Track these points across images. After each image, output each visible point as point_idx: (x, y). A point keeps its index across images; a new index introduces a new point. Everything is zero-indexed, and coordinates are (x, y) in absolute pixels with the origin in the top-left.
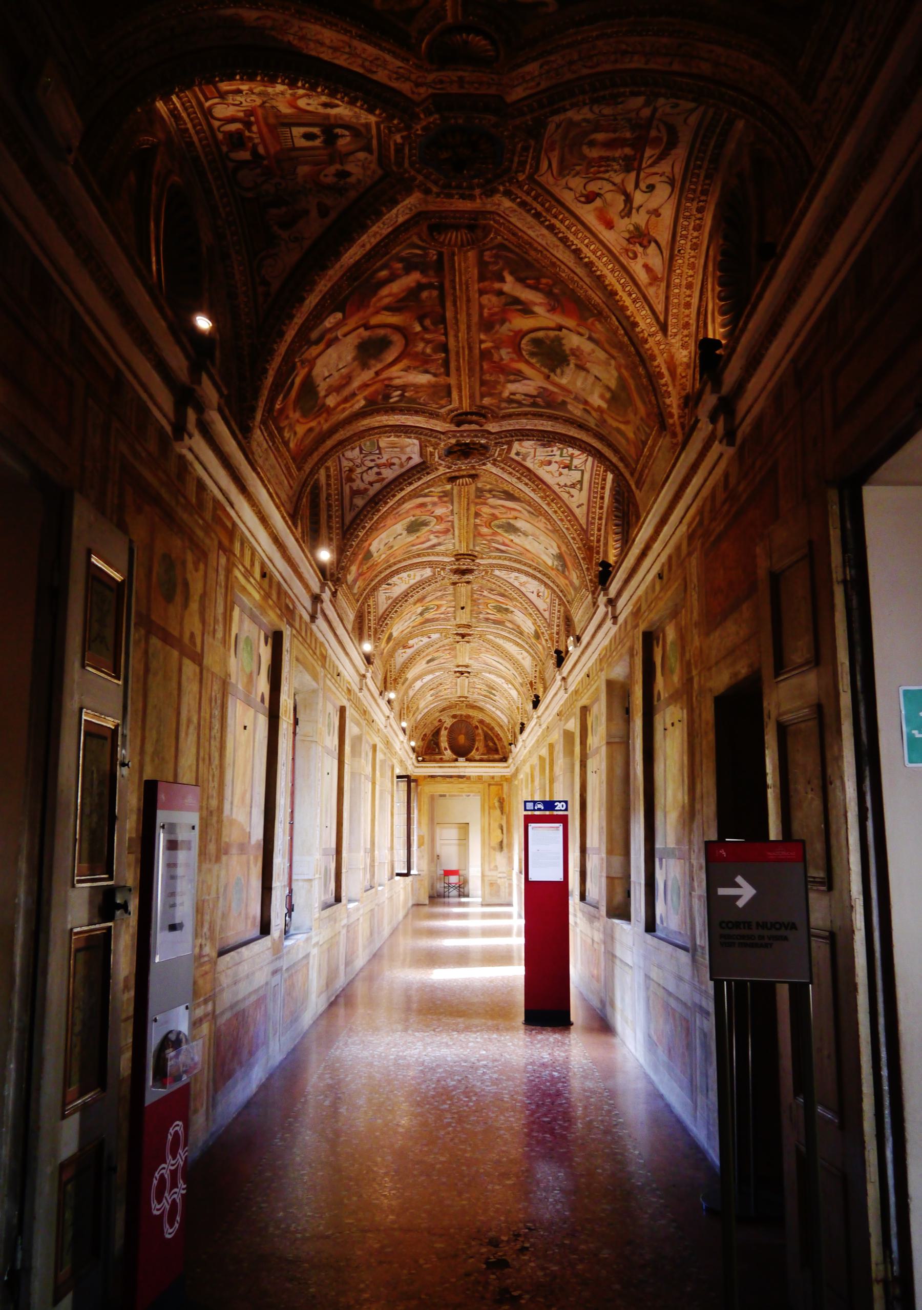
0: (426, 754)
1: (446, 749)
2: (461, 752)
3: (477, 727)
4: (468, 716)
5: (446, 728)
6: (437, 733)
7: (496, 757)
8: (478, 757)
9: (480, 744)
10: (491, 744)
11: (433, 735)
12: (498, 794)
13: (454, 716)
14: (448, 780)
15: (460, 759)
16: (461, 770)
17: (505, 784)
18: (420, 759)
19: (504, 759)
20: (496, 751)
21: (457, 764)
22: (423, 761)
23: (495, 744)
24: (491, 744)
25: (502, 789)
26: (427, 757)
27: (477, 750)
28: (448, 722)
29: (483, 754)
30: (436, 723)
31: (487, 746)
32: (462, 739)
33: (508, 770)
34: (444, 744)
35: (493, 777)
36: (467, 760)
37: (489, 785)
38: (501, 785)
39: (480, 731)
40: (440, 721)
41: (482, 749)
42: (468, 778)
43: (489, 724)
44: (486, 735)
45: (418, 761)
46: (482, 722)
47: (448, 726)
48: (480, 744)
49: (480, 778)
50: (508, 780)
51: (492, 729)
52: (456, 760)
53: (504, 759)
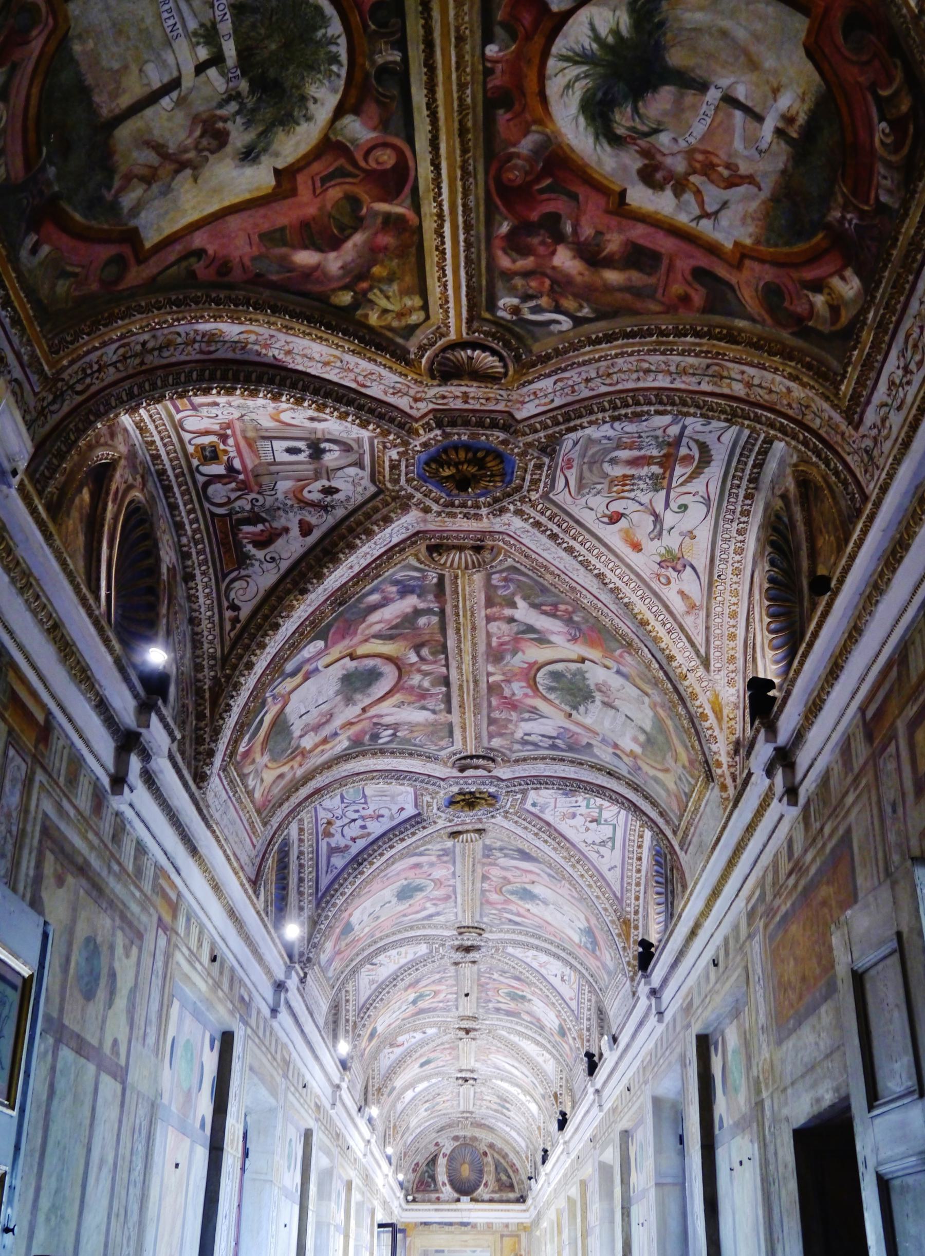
0: (418, 1191)
1: (444, 1184)
2: (465, 1189)
3: (485, 1154)
4: (474, 1139)
5: (445, 1155)
6: (433, 1162)
7: (512, 1196)
8: (486, 1197)
9: (489, 1177)
10: (504, 1178)
11: (428, 1164)
12: (514, 1250)
13: (456, 1138)
14: (447, 1228)
15: (464, 1199)
16: (465, 1214)
17: (523, 1236)
18: (410, 1198)
19: (522, 1199)
20: (511, 1187)
21: (459, 1206)
22: (414, 1200)
23: (509, 1177)
24: (504, 1178)
25: (519, 1242)
26: (419, 1196)
27: (486, 1185)
28: (448, 1147)
29: (493, 1192)
30: (432, 1148)
31: (498, 1180)
32: (466, 1171)
33: (527, 1215)
34: (442, 1176)
35: (507, 1226)
36: (472, 1200)
37: (502, 1236)
38: (518, 1236)
39: (489, 1159)
40: (437, 1144)
41: (492, 1184)
42: (474, 1226)
43: (501, 1149)
44: (497, 1165)
45: (408, 1201)
46: (491, 1146)
47: (448, 1152)
48: (489, 1177)
49: (489, 1226)
50: (526, 1228)
51: (505, 1156)
52: (458, 1200)
53: (522, 1199)
